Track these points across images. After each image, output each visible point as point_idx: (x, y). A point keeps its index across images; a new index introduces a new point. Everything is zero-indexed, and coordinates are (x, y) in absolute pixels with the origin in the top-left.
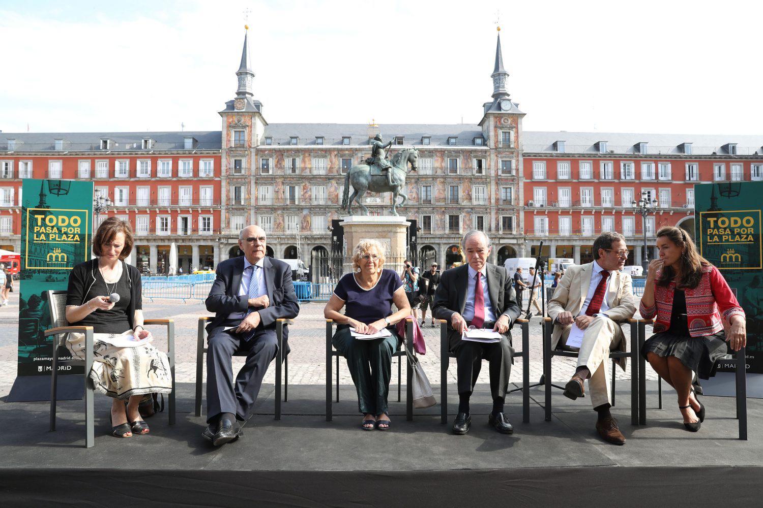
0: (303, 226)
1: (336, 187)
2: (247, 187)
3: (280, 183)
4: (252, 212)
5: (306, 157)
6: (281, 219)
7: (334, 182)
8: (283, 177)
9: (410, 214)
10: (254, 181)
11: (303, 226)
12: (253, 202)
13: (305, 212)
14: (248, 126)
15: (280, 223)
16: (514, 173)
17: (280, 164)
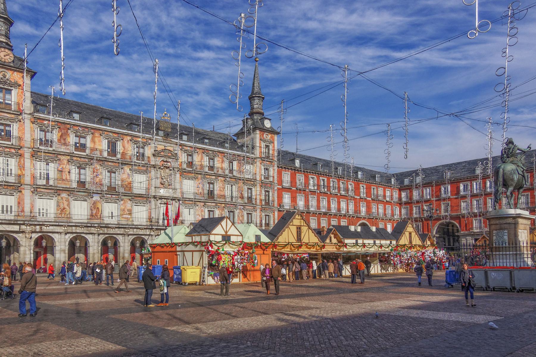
0: (92, 213)
1: (128, 174)
2: (18, 160)
3: (65, 162)
4: (27, 193)
5: (96, 137)
6: (66, 203)
7: (127, 169)
8: (68, 155)
9: (197, 207)
10: (30, 154)
11: (92, 213)
12: (27, 179)
13: (96, 198)
14: (20, 86)
15: (64, 208)
16: (271, 179)
17: (65, 139)
